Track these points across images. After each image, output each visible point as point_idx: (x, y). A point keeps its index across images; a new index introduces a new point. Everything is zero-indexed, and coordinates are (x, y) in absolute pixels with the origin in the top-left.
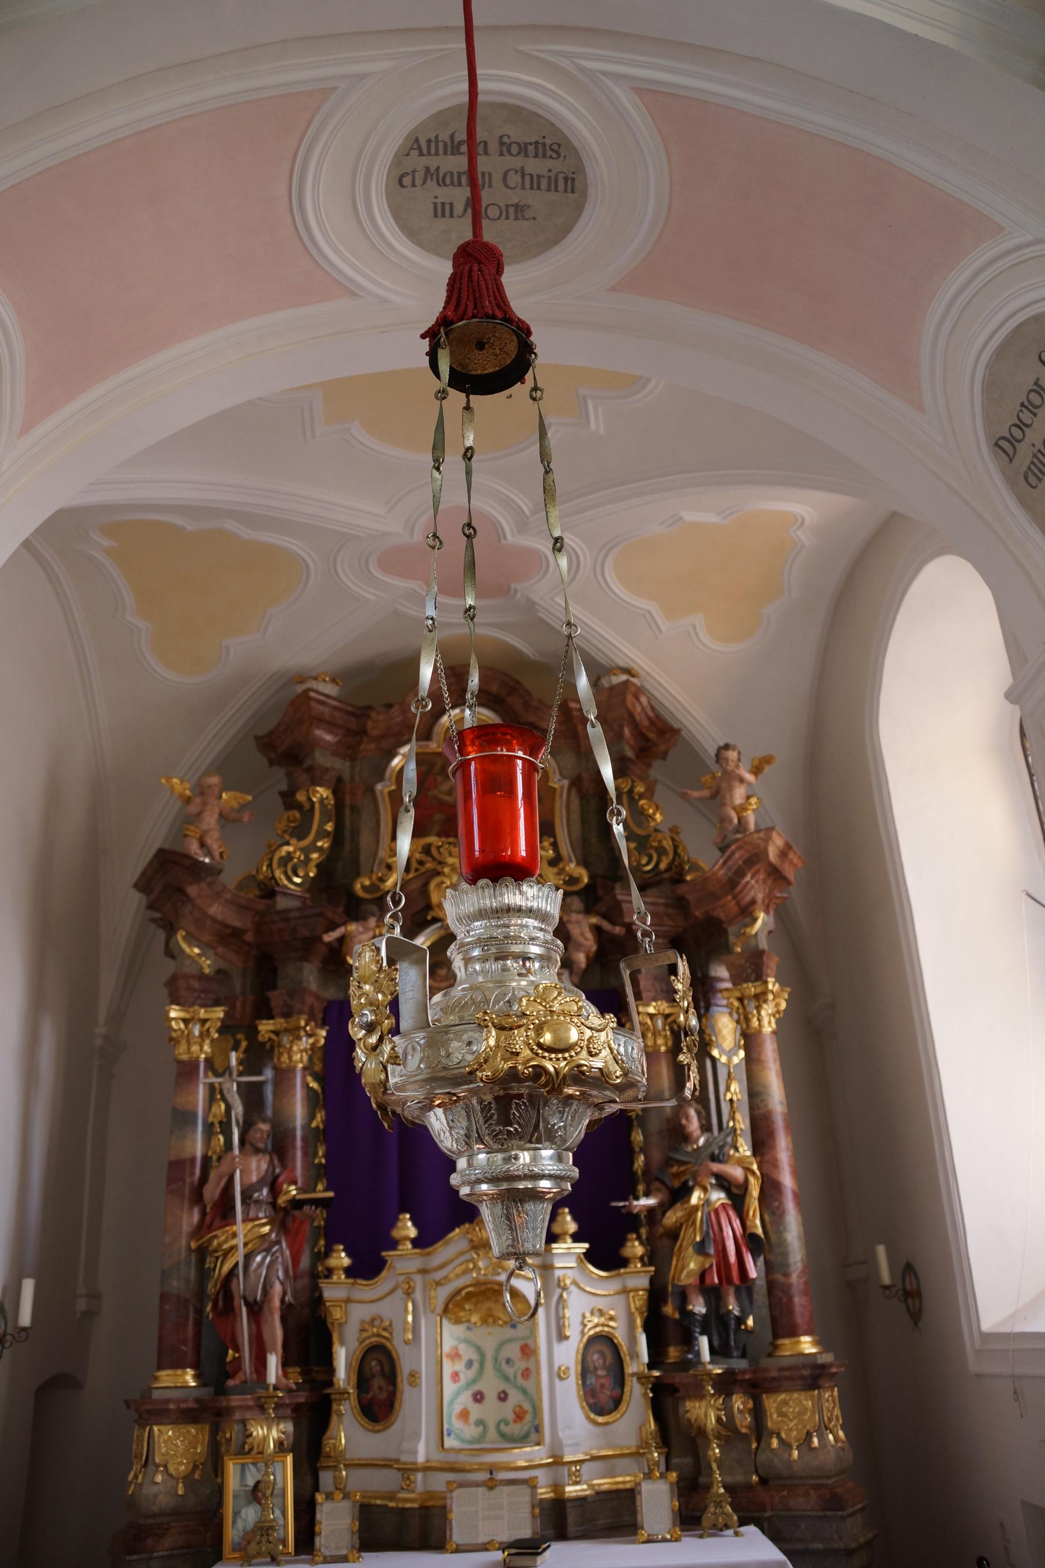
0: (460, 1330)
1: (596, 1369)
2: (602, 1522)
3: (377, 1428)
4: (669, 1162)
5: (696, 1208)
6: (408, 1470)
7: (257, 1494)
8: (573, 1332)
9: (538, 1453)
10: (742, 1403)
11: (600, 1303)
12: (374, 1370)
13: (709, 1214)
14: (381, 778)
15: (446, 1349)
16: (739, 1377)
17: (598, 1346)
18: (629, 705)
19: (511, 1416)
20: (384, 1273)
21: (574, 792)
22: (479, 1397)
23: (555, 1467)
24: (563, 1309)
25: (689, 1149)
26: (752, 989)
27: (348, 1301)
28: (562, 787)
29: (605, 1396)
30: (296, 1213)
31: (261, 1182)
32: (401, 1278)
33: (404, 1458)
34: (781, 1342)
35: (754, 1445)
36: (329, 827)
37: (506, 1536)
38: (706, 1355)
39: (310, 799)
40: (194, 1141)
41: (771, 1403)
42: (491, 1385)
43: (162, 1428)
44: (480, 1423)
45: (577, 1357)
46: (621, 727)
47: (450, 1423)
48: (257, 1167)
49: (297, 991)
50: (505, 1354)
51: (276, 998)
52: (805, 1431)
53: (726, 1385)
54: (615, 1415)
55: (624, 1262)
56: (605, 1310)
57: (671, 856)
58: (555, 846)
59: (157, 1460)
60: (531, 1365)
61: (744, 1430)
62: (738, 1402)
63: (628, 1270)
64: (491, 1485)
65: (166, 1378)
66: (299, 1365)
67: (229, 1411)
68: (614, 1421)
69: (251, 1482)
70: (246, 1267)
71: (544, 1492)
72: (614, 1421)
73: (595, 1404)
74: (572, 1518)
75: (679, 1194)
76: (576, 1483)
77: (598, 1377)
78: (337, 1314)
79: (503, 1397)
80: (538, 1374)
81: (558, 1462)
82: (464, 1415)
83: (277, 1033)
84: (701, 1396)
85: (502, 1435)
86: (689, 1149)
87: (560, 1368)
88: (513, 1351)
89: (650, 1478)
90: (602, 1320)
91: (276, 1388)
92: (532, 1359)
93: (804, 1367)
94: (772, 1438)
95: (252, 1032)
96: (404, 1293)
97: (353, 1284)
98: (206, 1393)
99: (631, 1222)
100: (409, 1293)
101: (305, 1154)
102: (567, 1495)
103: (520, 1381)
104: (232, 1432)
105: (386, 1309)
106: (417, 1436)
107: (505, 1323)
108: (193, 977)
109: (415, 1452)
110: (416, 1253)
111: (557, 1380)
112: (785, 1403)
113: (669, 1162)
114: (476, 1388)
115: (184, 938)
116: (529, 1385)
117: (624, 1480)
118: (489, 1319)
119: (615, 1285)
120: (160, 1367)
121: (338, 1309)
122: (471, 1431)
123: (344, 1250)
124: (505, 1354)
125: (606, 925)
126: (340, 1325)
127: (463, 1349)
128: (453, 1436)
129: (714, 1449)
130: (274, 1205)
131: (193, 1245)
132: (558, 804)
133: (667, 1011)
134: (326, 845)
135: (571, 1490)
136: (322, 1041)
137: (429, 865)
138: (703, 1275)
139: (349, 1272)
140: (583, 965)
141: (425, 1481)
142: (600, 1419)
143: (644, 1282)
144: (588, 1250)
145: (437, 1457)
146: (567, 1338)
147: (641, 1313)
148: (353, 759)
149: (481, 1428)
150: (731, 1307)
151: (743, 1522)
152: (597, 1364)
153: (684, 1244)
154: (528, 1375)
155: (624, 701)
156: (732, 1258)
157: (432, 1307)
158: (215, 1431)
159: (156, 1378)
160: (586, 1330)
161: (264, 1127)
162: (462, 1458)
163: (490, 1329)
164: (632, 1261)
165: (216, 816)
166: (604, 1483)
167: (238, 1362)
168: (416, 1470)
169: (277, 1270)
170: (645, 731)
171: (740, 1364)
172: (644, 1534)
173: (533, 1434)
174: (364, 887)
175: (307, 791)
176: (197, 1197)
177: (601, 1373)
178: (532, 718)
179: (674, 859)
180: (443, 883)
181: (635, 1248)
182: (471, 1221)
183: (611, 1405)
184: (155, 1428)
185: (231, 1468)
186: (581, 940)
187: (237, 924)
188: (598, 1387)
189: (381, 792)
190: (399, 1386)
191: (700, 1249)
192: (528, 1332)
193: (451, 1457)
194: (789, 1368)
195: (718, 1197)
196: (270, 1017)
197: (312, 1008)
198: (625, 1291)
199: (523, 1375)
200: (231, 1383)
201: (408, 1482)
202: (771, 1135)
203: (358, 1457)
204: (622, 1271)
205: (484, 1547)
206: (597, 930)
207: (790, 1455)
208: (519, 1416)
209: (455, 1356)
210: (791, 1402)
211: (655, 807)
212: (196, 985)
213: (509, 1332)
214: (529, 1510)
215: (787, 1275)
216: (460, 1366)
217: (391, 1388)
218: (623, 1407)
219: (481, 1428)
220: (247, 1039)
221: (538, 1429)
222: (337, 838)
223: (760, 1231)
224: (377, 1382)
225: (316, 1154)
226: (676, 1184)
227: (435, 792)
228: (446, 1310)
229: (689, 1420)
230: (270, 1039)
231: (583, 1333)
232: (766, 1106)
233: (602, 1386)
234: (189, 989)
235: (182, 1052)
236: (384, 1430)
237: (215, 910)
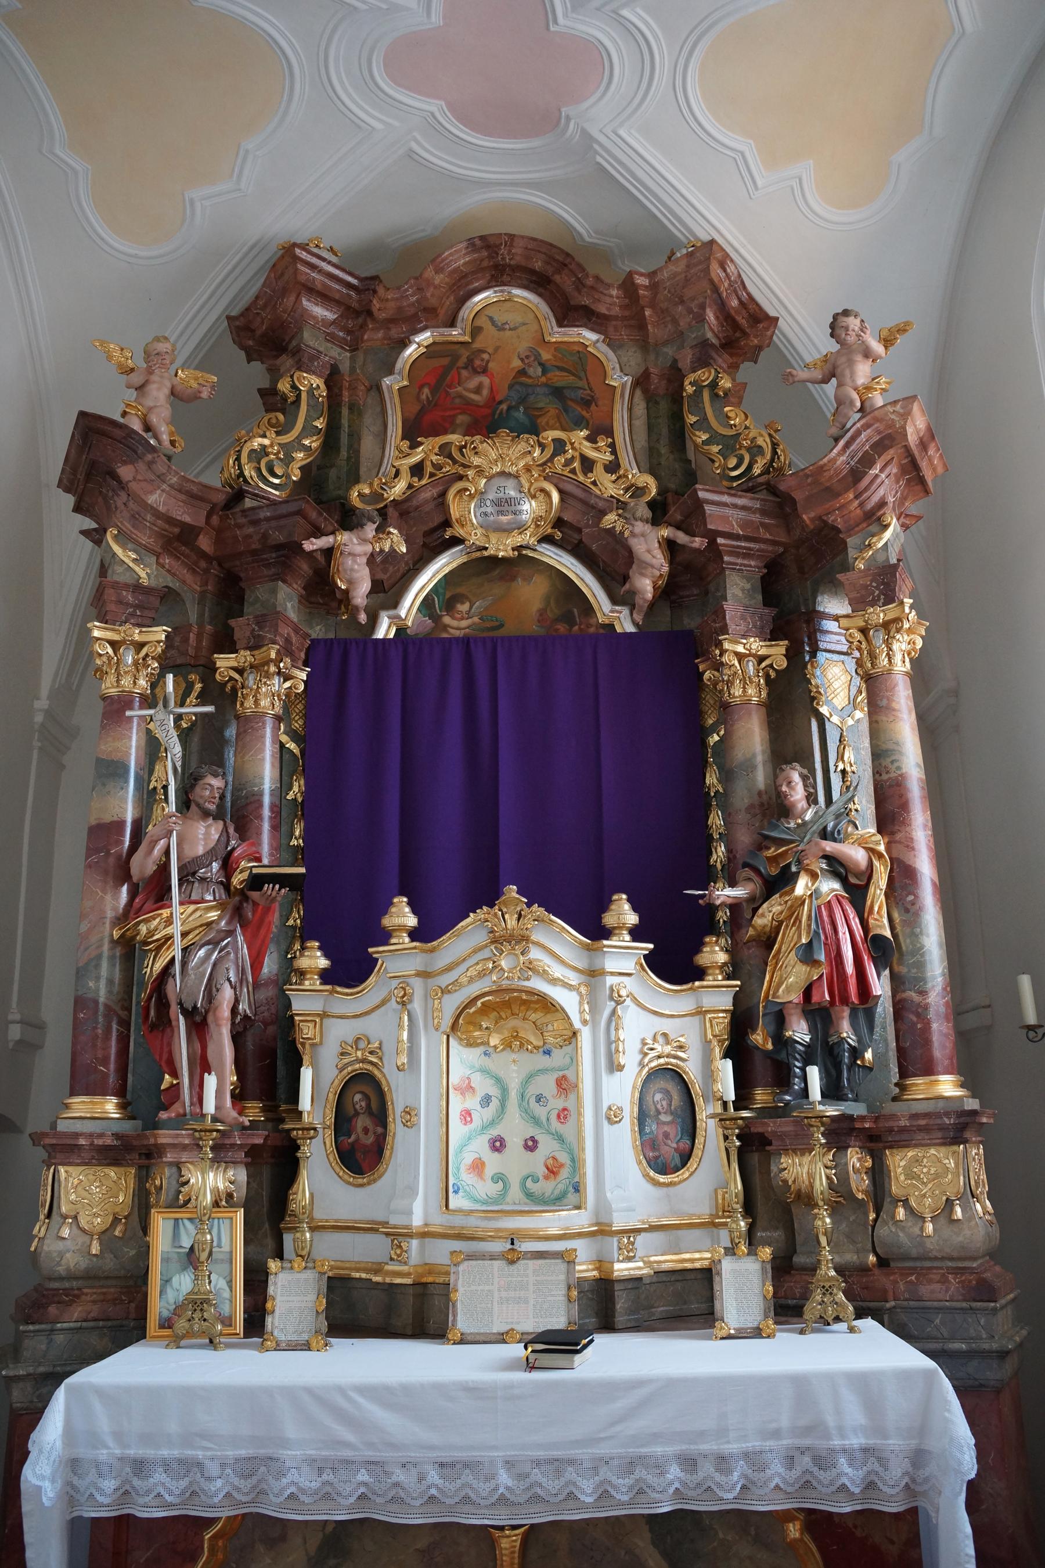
0: (473, 1055)
1: (658, 1113)
2: (661, 1310)
3: (360, 1181)
4: (764, 842)
6: (398, 1236)
7: (192, 1259)
8: (630, 1059)
10: (859, 1160)
12: (357, 1107)
13: (819, 907)
14: (390, 372)
15: (454, 1079)
16: (858, 1125)
17: (662, 1083)
18: (713, 275)
19: (541, 1171)
20: (372, 979)
21: (638, 393)
22: (498, 1145)
23: (600, 1237)
24: (617, 1029)
25: (792, 825)
26: (879, 614)
27: (324, 1015)
28: (624, 385)
29: (669, 1150)
30: (255, 895)
31: (211, 854)
32: (395, 983)
33: (393, 1221)
34: (909, 1082)
35: (872, 1216)
36: (320, 424)
37: (533, 1325)
38: (815, 1091)
39: (294, 387)
40: (124, 800)
41: (898, 1162)
42: (515, 1130)
43: (70, 1169)
44: (499, 1178)
45: (633, 1096)
46: (703, 307)
47: (457, 1176)
49: (269, 618)
50: (532, 1090)
51: (241, 627)
52: (944, 1198)
54: (684, 1173)
55: (700, 973)
56: (671, 1036)
57: (768, 456)
58: (613, 446)
59: (64, 1209)
60: (570, 1104)
61: (860, 1196)
62: (855, 1158)
63: (705, 983)
64: (512, 1258)
65: (81, 1106)
66: (261, 1100)
68: (680, 1182)
69: (186, 1243)
70: (184, 964)
71: (585, 1270)
72: (680, 1182)
73: (657, 1158)
74: (621, 1304)
76: (629, 1259)
77: (660, 1123)
78: (307, 1031)
79: (531, 1145)
80: (580, 1114)
81: (602, 1231)
82: (478, 1167)
83: (240, 671)
84: (804, 1147)
85: (529, 1195)
86: (792, 825)
87: (610, 1108)
88: (547, 1085)
89: (734, 1254)
90: (668, 1049)
91: (215, 1119)
92: (572, 1097)
93: (947, 1114)
94: (897, 1207)
96: (398, 1003)
97: (332, 992)
98: (128, 1127)
100: (404, 1003)
101: (275, 827)
102: (616, 1274)
103: (555, 1124)
104: (163, 1178)
105: (375, 1027)
107: (537, 1048)
108: (126, 586)
109: (410, 1213)
110: (415, 948)
111: (605, 1123)
112: (917, 1161)
113: (764, 842)
114: (495, 1132)
115: (116, 538)
116: (567, 1130)
117: (697, 1257)
118: (513, 1042)
120: (73, 1093)
121: (311, 1025)
122: (487, 1188)
123: (320, 948)
124: (532, 1090)
125: (681, 538)
126: (313, 1045)
127: (477, 1079)
128: (461, 1193)
129: (823, 1219)
130: (227, 886)
131: (116, 934)
132: (617, 406)
133: (763, 652)
134: (314, 445)
135: (621, 1269)
136: (302, 687)
138: (807, 993)
139: (326, 977)
140: (649, 596)
141: (422, 1249)
142: (662, 1179)
143: (724, 1001)
144: (652, 952)
145: (439, 1221)
146: (620, 1068)
147: (721, 1042)
148: (354, 349)
149: (500, 1184)
150: (845, 1035)
151: (860, 1315)
152: (659, 1106)
153: (783, 949)
154: (565, 1117)
155: (707, 270)
156: (850, 968)
157: (436, 1021)
158: (144, 1175)
159: (67, 1107)
160: (646, 1060)
162: (473, 1222)
163: (514, 1056)
164: (710, 971)
165: (166, 391)
166: (668, 1261)
167: (175, 1090)
168: (410, 1236)
169: (227, 969)
170: (733, 312)
171: (857, 1109)
172: (721, 1329)
174: (360, 495)
175: (292, 377)
176: (123, 873)
177: (664, 1118)
178: (586, 301)
179: (772, 460)
180: (466, 490)
182: (491, 905)
183: (677, 1160)
184: (62, 1170)
185: (161, 1225)
186: (648, 558)
187: (187, 519)
188: (661, 1137)
189: (390, 388)
190: (391, 1127)
191: (807, 955)
192: (568, 1060)
193: (458, 1221)
194: (926, 1115)
195: (830, 886)
197: (288, 641)
198: (700, 1012)
199: (559, 1116)
200: (163, 1115)
201: (398, 1251)
202: (905, 806)
203: (335, 1217)
204: (697, 983)
205: (502, 1339)
206: (670, 546)
207: (922, 1229)
208: (552, 1171)
209: (467, 1089)
210: (925, 1160)
211: (743, 416)
213: (544, 1061)
214: (564, 1292)
215: (923, 993)
216: (472, 1103)
217: (380, 1130)
218: (693, 1164)
219: (500, 1184)
220: (202, 681)
221: (577, 1189)
223: (887, 933)
224: (362, 1122)
225: (291, 834)
226: (774, 871)
227: (459, 389)
228: (454, 1026)
229: (785, 1181)
230: (231, 679)
231: (641, 1064)
232: (899, 768)
233: (666, 1135)
234: (120, 602)
235: (109, 687)
236: (369, 1183)
237: (156, 499)
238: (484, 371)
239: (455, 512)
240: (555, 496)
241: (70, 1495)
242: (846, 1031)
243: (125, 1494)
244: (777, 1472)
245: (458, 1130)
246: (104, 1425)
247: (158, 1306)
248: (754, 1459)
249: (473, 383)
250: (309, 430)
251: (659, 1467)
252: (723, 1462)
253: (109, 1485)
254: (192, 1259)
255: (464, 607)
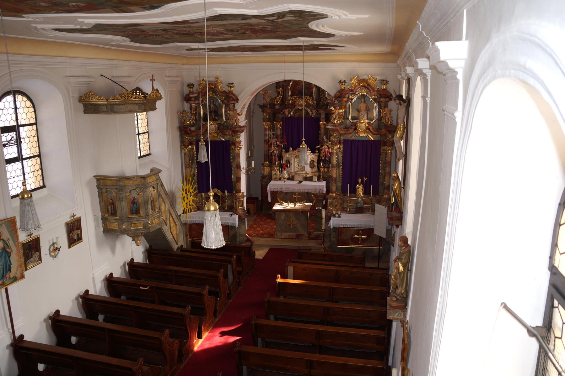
5: (323, 148)
7: (275, 174)
9: (304, 172)
11: (313, 157)
15: (295, 161)
17: (312, 161)
22: (299, 166)
31: (275, 142)
36: (282, 94)
48: (274, 141)
53: (324, 167)
55: (316, 153)
64: (299, 175)
67: (272, 166)
71: (304, 176)
75: (322, 146)
81: (306, 173)
82: (297, 168)
95: (273, 123)
99: (316, 149)
100: (291, 155)
104: (273, 168)
106: (292, 170)
119: (314, 155)
125: (317, 112)
130: (276, 145)
135: (307, 176)
137: (295, 100)
138: (324, 155)
139: (285, 152)
143: (318, 155)
145: (294, 172)
151: (324, 180)
156: (327, 154)
158: (271, 168)
161: (275, 136)
166: (311, 175)
173: (304, 170)
174: (287, 103)
181: (317, 151)
185: (273, 172)
196: (275, 121)
200: (272, 163)
205: (297, 181)
209: (296, 162)
212: (266, 119)
221: (304, 169)
222: (283, 95)
226: (322, 145)
227: (297, 87)
228: (295, 157)
237: (268, 111)
238: (299, 85)
239: (296, 105)
240: (306, 103)
241: (270, 190)
242: (327, 159)
243: (273, 190)
244: (313, 190)
245: (295, 165)
246: (272, 186)
247: (273, 178)
248: (312, 190)
249: (298, 87)
250: (281, 95)
251: (306, 190)
252: (310, 190)
253: (272, 189)
254: (275, 174)
255: (297, 113)
